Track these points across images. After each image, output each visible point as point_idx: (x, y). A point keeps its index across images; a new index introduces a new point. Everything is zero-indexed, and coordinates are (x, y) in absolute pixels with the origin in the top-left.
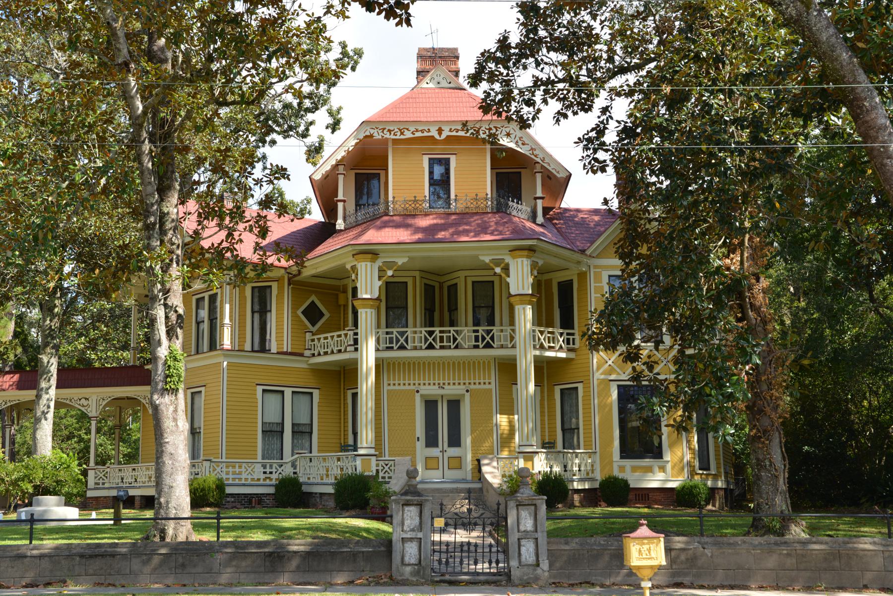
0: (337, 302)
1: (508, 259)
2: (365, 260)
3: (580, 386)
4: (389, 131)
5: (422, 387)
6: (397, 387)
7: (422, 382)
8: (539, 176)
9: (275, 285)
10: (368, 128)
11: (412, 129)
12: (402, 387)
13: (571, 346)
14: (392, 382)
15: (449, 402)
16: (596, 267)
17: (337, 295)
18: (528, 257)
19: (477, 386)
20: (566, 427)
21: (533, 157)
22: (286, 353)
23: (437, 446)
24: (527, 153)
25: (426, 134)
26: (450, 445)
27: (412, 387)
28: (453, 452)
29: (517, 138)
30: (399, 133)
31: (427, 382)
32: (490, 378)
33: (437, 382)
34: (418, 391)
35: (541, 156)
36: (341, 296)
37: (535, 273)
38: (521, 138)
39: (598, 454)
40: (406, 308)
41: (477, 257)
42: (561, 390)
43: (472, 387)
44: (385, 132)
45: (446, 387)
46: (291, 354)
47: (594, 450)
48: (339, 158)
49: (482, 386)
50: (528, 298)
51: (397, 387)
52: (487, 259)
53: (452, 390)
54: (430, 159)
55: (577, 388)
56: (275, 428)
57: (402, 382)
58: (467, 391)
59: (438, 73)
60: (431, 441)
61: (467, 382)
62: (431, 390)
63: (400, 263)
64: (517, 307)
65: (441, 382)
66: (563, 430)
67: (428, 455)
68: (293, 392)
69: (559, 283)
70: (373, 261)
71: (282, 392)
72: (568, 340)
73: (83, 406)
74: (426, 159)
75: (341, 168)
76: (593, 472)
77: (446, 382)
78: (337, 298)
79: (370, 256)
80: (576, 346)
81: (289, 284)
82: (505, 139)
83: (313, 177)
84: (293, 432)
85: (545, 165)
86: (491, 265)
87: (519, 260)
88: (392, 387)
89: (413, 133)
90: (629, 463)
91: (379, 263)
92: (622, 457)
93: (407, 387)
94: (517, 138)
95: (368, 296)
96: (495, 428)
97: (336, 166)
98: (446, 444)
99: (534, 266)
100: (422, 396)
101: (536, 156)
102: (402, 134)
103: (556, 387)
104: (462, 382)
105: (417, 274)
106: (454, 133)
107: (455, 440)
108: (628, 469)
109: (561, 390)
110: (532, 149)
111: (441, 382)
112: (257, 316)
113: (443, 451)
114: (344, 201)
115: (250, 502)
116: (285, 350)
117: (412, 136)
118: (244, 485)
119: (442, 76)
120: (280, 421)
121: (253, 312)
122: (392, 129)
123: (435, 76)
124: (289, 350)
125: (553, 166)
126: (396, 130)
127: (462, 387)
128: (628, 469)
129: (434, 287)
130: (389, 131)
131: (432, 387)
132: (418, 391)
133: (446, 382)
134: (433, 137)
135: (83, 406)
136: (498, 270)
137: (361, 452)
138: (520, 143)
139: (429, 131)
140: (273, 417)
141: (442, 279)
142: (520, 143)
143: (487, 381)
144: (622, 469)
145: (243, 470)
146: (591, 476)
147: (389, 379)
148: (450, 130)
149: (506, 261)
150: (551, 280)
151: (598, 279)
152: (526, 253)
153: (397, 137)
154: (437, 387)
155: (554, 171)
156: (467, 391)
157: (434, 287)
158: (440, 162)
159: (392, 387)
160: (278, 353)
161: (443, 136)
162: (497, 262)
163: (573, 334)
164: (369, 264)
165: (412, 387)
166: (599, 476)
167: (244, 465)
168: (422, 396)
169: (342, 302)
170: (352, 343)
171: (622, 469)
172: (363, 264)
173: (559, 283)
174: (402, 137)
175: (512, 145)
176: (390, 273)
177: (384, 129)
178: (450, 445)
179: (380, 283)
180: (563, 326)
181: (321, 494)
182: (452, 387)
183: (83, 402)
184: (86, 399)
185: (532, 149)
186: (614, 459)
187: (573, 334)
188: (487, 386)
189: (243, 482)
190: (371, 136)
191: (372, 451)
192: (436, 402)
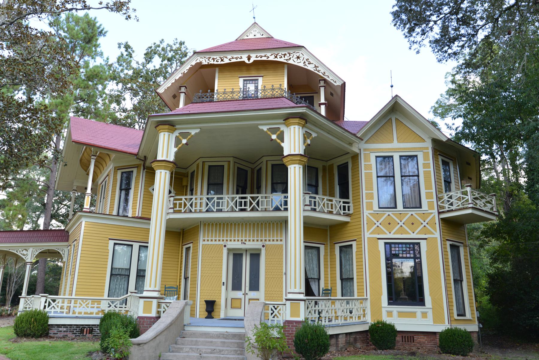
0: (182, 184)
1: (283, 128)
3: (354, 243)
4: (214, 59)
5: (229, 243)
6: (210, 243)
7: (229, 239)
8: (322, 90)
9: (135, 170)
10: (199, 58)
11: (229, 57)
12: (214, 243)
13: (347, 211)
14: (206, 239)
15: (252, 255)
16: (365, 150)
17: (182, 179)
18: (299, 124)
19: (271, 243)
20: (344, 277)
21: (316, 72)
22: (137, 218)
23: (239, 289)
24: (312, 70)
25: (239, 60)
26: (251, 289)
27: (221, 243)
28: (253, 294)
30: (220, 60)
31: (233, 239)
32: (281, 236)
33: (240, 239)
34: (225, 246)
35: (322, 71)
36: (185, 180)
37: (309, 142)
39: (369, 301)
40: (222, 184)
41: (256, 127)
42: (340, 247)
43: (268, 243)
44: (210, 60)
45: (247, 243)
46: (141, 218)
47: (365, 297)
48: (177, 78)
49: (275, 243)
50: (298, 158)
51: (210, 243)
52: (265, 128)
53: (251, 245)
55: (351, 245)
56: (123, 273)
57: (210, 239)
58: (263, 246)
59: (255, 29)
60: (237, 286)
61: (264, 239)
62: (236, 245)
63: (193, 134)
64: (289, 167)
65: (244, 239)
66: (342, 279)
67: (233, 297)
68: (140, 246)
69: (338, 166)
71: (132, 246)
72: (344, 207)
73: (24, 255)
74: (241, 80)
75: (183, 89)
76: (364, 316)
77: (248, 239)
78: (182, 181)
79: (167, 127)
80: (351, 212)
81: (144, 169)
84: (137, 276)
86: (269, 133)
87: (292, 127)
88: (206, 243)
89: (230, 60)
90: (396, 309)
92: (389, 304)
93: (217, 243)
94: (305, 60)
96: (284, 276)
98: (247, 288)
99: (306, 136)
100: (229, 250)
101: (318, 71)
102: (222, 60)
103: (336, 245)
104: (260, 239)
105: (231, 159)
106: (259, 59)
107: (254, 286)
108: (395, 314)
109: (340, 247)
110: (316, 67)
111: (244, 239)
112: (123, 192)
113: (245, 294)
115: (82, 331)
116: (137, 215)
118: (77, 318)
119: (257, 31)
120: (128, 268)
121: (121, 190)
122: (215, 57)
124: (140, 215)
125: (331, 78)
126: (218, 58)
128: (395, 314)
129: (247, 171)
130: (214, 59)
131: (236, 243)
132: (225, 246)
133: (248, 239)
135: (24, 255)
136: (274, 137)
137: (145, 294)
138: (307, 63)
139: (241, 58)
140: (121, 263)
141: (253, 166)
142: (307, 63)
143: (279, 239)
144: (390, 314)
145: (78, 305)
146: (362, 319)
147: (204, 236)
148: (256, 57)
149: (282, 129)
150: (333, 164)
151: (368, 159)
152: (297, 120)
153: (219, 63)
154: (240, 242)
155: (332, 81)
156: (263, 246)
157: (247, 171)
159: (206, 243)
160: (132, 217)
161: (251, 61)
162: (274, 131)
163: (348, 203)
165: (221, 243)
166: (370, 320)
167: (79, 301)
168: (229, 250)
169: (184, 184)
170: (172, 206)
171: (390, 314)
173: (338, 166)
174: (222, 63)
175: (301, 65)
176: (184, 141)
177: (210, 58)
178: (251, 289)
179: (176, 149)
180: (341, 197)
182: (251, 243)
183: (25, 252)
184: (26, 250)
185: (316, 67)
186: (383, 306)
187: (348, 203)
188: (279, 243)
189: (77, 315)
190: (201, 63)
191: (155, 294)
192: (241, 255)
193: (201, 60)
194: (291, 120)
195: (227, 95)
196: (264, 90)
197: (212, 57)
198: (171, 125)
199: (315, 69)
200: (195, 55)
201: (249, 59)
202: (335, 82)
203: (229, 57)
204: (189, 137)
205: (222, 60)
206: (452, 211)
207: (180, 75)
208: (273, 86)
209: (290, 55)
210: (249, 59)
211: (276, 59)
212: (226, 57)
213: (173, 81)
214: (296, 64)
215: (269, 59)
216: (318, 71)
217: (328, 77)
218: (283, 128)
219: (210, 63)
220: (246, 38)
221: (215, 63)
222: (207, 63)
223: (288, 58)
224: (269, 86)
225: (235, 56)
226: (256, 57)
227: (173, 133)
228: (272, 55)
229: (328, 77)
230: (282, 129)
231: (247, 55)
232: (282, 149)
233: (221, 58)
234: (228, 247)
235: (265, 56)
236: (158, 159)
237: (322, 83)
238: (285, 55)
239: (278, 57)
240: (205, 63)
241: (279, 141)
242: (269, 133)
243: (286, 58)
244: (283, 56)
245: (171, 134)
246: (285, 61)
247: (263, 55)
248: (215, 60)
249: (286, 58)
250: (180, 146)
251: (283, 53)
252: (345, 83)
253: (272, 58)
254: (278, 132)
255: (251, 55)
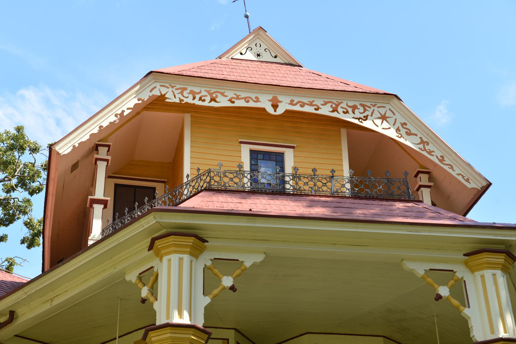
1: (461, 272)
2: (178, 249)
10: (158, 85)
11: (230, 94)
21: (424, 153)
25: (252, 104)
29: (398, 124)
30: (208, 99)
38: (403, 124)
44: (185, 94)
48: (105, 124)
52: (420, 269)
54: (252, 152)
59: (258, 42)
63: (248, 264)
70: (196, 253)
75: (103, 152)
82: (378, 122)
83: (57, 148)
85: (446, 168)
86: (429, 280)
87: (488, 273)
91: (206, 259)
94: (398, 124)
95: (186, 320)
97: (95, 146)
105: (231, 335)
106: (297, 108)
110: (422, 142)
114: (104, 203)
117: (230, 104)
119: (264, 47)
122: (197, 90)
123: (253, 46)
126: (204, 93)
134: (264, 109)
136: (444, 291)
138: (403, 131)
139: (257, 100)
148: (292, 103)
149: (459, 275)
152: (501, 259)
153: (206, 104)
155: (460, 178)
158: (268, 156)
161: (280, 111)
164: (186, 258)
172: (175, 258)
174: (213, 104)
175: (392, 133)
176: (227, 281)
177: (186, 89)
179: (207, 300)
185: (422, 142)
190: (162, 98)
193: (164, 91)
194: (485, 257)
195: (319, 184)
196: (295, 176)
197: (190, 88)
198: (196, 239)
199: (421, 146)
200: (150, 77)
201: (275, 107)
202: (467, 180)
203: (230, 94)
204: (238, 272)
205: (213, 100)
207: (113, 119)
208: (314, 170)
209: (365, 110)
210: (275, 107)
211: (335, 115)
212: (223, 94)
213: (96, 131)
214: (379, 130)
215: (319, 112)
216: (430, 152)
217: (452, 168)
218: (461, 272)
219: (186, 100)
220: (239, 56)
221: (197, 102)
222: (177, 101)
223: (362, 116)
224: (305, 170)
225: (243, 95)
226: (292, 103)
227: (197, 257)
228: (325, 104)
229: (452, 168)
230: (459, 275)
231: (270, 97)
232: (464, 325)
233: (211, 94)
235: (311, 104)
236: (158, 323)
237: (424, 179)
238: (354, 108)
239: (340, 110)
240: (172, 97)
241: (455, 302)
242: (429, 280)
243: (357, 114)
244: (350, 110)
245: (194, 259)
246: (356, 122)
247: (306, 100)
248: (197, 97)
249: (357, 114)
250: (215, 292)
251: (351, 104)
252: (490, 184)
253: (325, 111)
254: (452, 282)
255: (280, 98)
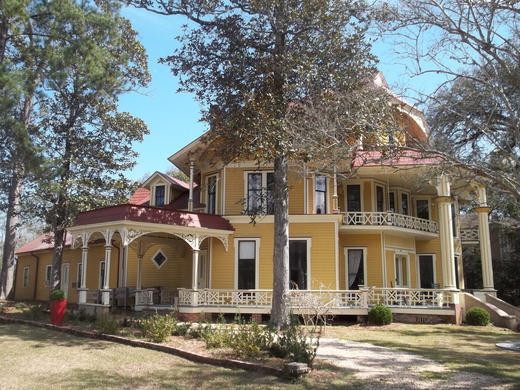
5: (396, 250)
27: (392, 250)
43: (410, 252)
53: (404, 253)
62: (398, 252)
88: (387, 249)
100: (396, 255)
127: (407, 251)
154: (399, 250)
159: (387, 249)
165: (392, 250)
168: (396, 255)
181: (397, 314)
206: (468, 241)
234: (396, 253)
